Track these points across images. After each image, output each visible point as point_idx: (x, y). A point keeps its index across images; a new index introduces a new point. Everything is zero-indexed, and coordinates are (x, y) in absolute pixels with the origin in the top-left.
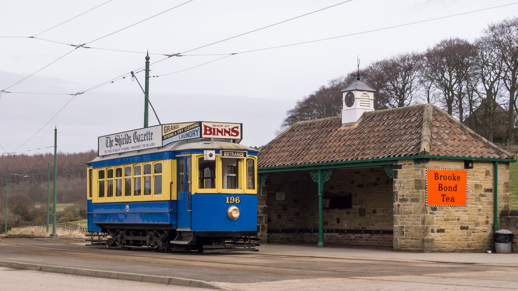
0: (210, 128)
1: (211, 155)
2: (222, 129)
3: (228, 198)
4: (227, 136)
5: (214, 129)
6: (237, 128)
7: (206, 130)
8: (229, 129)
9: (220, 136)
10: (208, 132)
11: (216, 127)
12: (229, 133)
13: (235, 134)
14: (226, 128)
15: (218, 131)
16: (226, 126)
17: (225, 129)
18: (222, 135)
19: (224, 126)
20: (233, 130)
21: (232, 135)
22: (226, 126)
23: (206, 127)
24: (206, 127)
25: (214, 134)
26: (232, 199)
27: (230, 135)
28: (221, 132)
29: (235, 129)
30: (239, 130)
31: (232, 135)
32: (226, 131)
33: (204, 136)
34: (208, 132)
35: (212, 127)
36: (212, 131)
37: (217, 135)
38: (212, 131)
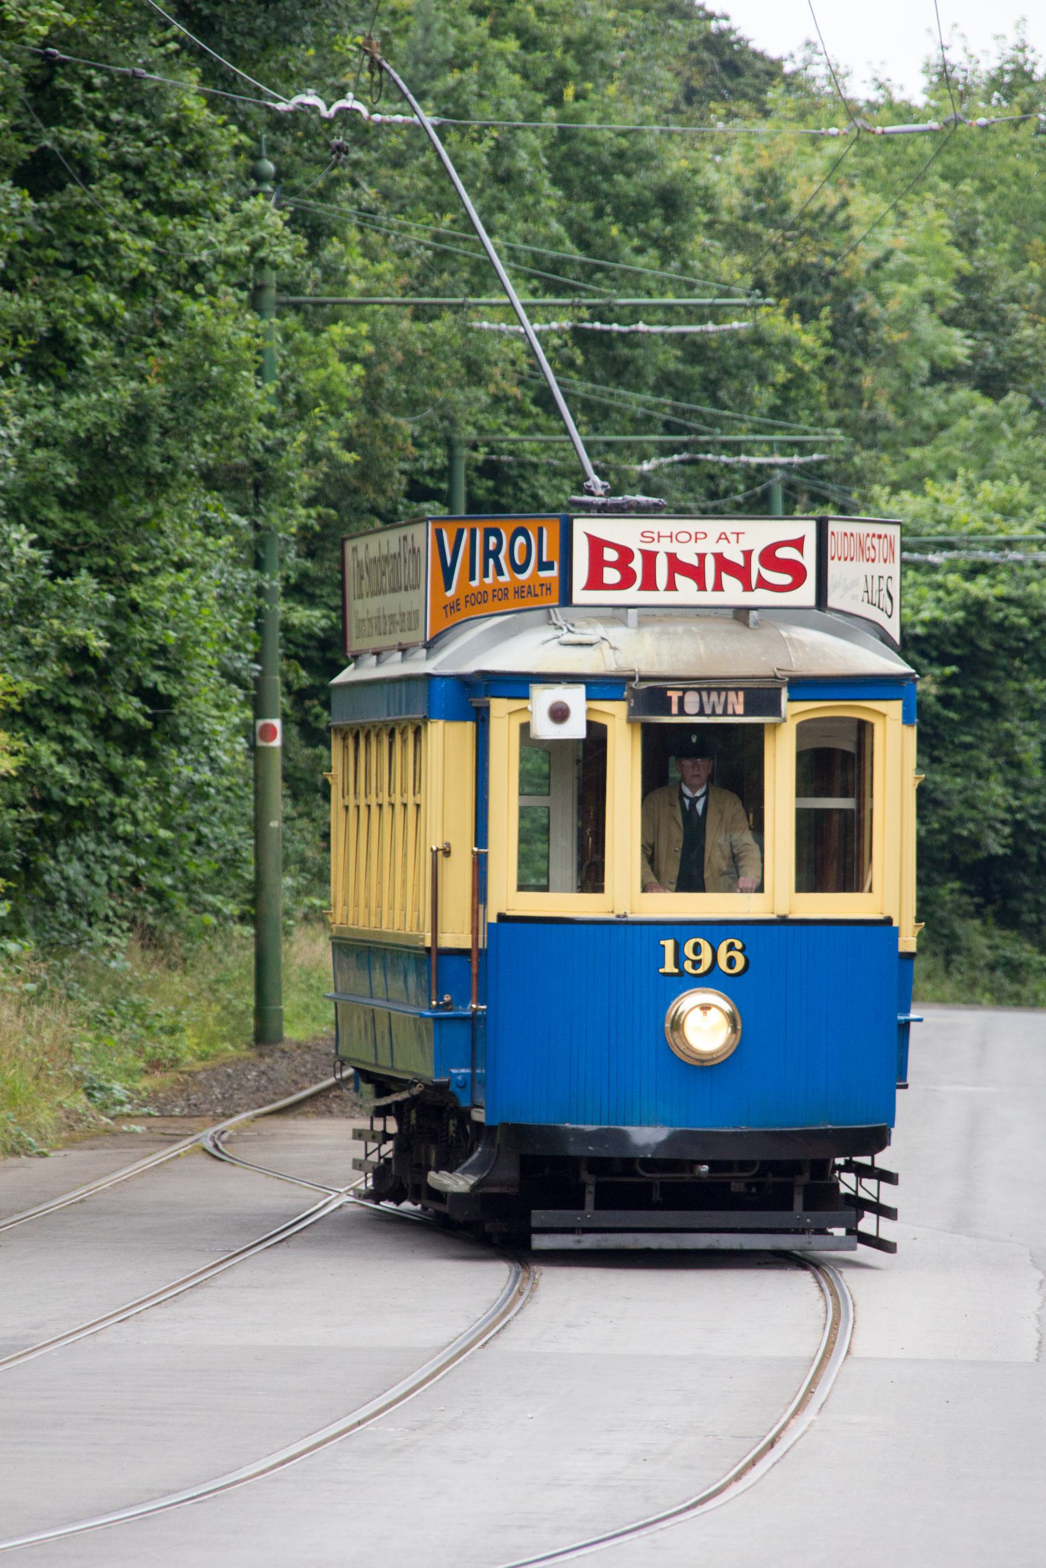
0: (626, 554)
2: (702, 557)
3: (669, 945)
5: (649, 558)
6: (798, 544)
7: (597, 564)
10: (611, 576)
11: (662, 548)
12: (742, 573)
13: (786, 579)
14: (723, 548)
15: (675, 565)
16: (723, 537)
17: (719, 557)
18: (702, 587)
19: (713, 536)
20: (769, 558)
21: (763, 584)
22: (723, 537)
23: (597, 545)
24: (597, 545)
25: (649, 584)
26: (697, 948)
28: (696, 574)
29: (783, 553)
30: (809, 560)
31: (763, 584)
32: (723, 564)
34: (611, 576)
35: (635, 544)
36: (637, 565)
37: (671, 586)
38: (637, 565)
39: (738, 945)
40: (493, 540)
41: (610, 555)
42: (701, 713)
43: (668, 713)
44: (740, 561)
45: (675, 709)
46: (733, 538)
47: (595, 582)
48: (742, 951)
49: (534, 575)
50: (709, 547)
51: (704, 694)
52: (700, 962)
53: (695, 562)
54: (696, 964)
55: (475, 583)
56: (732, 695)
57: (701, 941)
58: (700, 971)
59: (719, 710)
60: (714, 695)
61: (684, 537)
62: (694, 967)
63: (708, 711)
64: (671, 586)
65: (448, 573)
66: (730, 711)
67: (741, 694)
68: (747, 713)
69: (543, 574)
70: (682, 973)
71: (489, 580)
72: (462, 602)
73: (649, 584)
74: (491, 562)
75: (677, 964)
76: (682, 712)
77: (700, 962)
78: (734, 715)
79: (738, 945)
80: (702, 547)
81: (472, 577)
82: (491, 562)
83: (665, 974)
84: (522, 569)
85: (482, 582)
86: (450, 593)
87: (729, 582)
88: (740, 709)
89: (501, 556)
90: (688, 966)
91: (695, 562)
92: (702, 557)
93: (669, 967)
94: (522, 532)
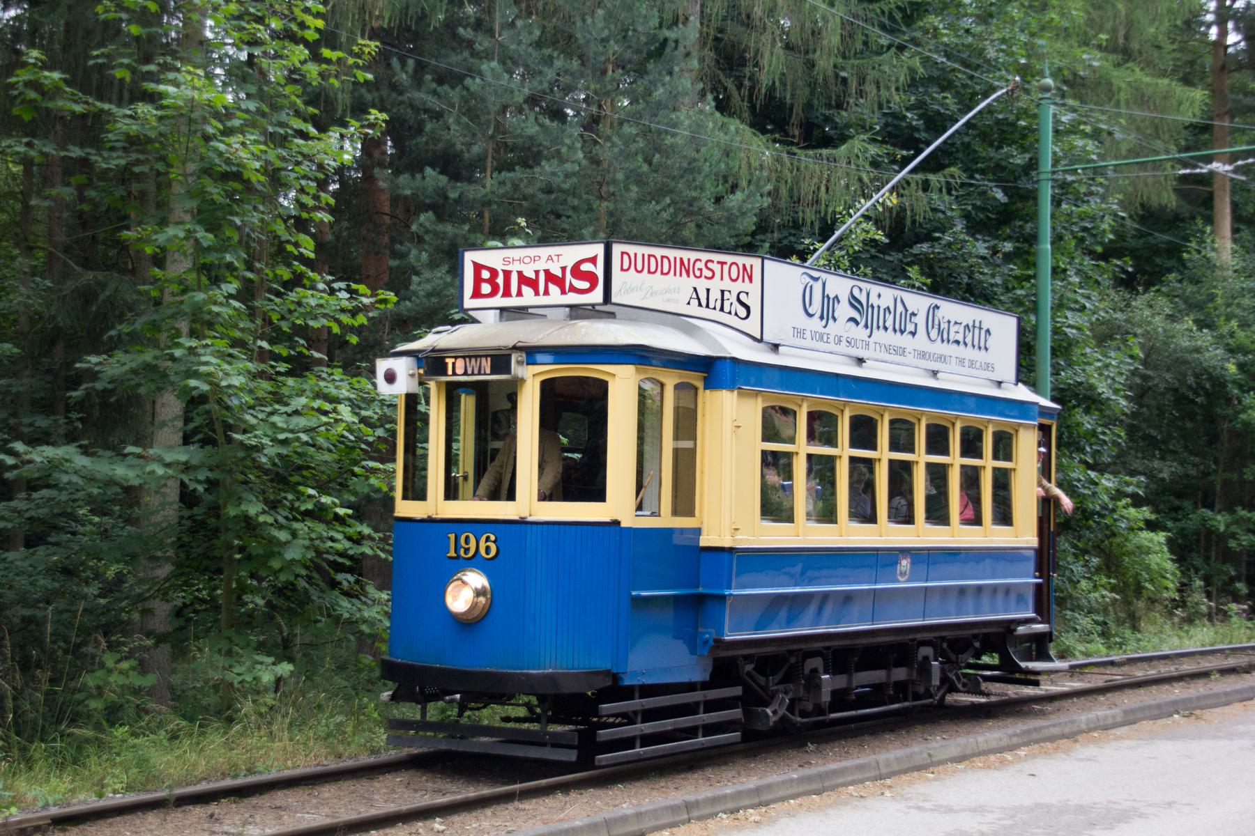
0: (494, 272)
2: (537, 272)
3: (452, 536)
5: (507, 274)
6: (593, 260)
7: (478, 280)
8: (564, 269)
10: (486, 288)
11: (514, 268)
12: (559, 282)
13: (584, 285)
15: (523, 279)
16: (550, 258)
17: (547, 272)
18: (537, 293)
19: (544, 258)
20: (577, 272)
21: (573, 289)
22: (550, 258)
23: (478, 268)
24: (478, 268)
25: (507, 293)
27: (563, 292)
28: (533, 284)
31: (573, 289)
32: (550, 277)
34: (486, 288)
35: (499, 267)
36: (500, 280)
37: (519, 294)
38: (500, 280)
39: (493, 538)
41: (486, 275)
42: (465, 374)
45: (450, 372)
46: (555, 258)
47: (477, 294)
48: (495, 542)
50: (541, 265)
54: (467, 550)
56: (484, 359)
57: (471, 536)
58: (470, 555)
68: (492, 374)
70: (458, 557)
73: (507, 293)
79: (493, 538)
83: (451, 558)
87: (553, 288)
88: (488, 371)
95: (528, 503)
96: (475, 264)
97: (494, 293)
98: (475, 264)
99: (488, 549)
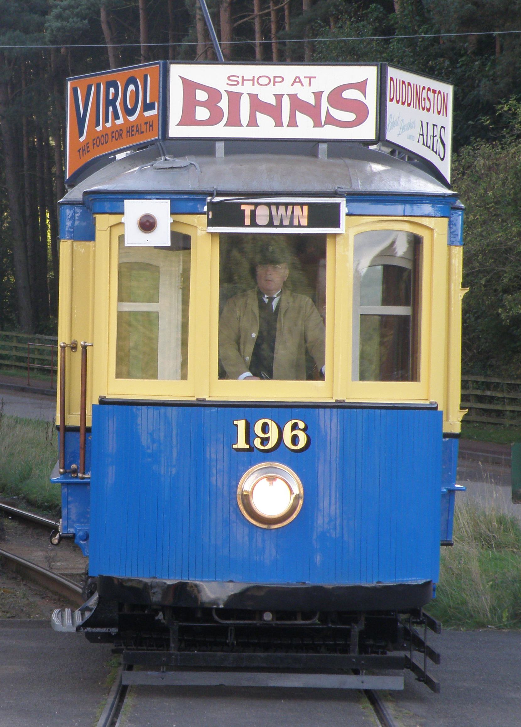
0: (214, 94)
1: (147, 225)
2: (279, 97)
3: (241, 425)
4: (305, 129)
5: (234, 98)
6: (361, 86)
8: (318, 95)
9: (266, 129)
10: (202, 113)
11: (246, 89)
12: (313, 111)
13: (350, 117)
14: (297, 89)
15: (257, 105)
16: (297, 80)
17: (293, 98)
18: (279, 123)
19: (289, 79)
20: (336, 98)
21: (331, 120)
22: (297, 80)
23: (190, 87)
24: (190, 87)
25: (234, 121)
27: (318, 124)
28: (274, 111)
29: (348, 94)
31: (331, 120)
32: (297, 104)
33: (176, 131)
34: (202, 113)
35: (222, 86)
36: (224, 104)
37: (253, 122)
38: (224, 104)
39: (301, 425)
40: (112, 90)
41: (201, 96)
42: (271, 224)
43: (242, 225)
44: (312, 100)
45: (247, 221)
46: (306, 81)
47: (188, 119)
48: (304, 430)
49: (141, 114)
50: (285, 89)
51: (273, 208)
52: (268, 439)
53: (273, 102)
54: (265, 441)
55: (99, 129)
56: (297, 209)
57: (269, 421)
58: (269, 447)
59: (286, 222)
60: (282, 209)
61: (264, 81)
62: (262, 444)
63: (276, 223)
64: (253, 122)
65: (81, 122)
66: (296, 223)
67: (306, 208)
68: (310, 225)
69: (147, 114)
70: (252, 449)
71: (109, 125)
72: (91, 145)
73: (234, 121)
74: (111, 109)
75: (248, 441)
76: (254, 224)
77: (268, 439)
78: (299, 226)
79: (301, 425)
80: (280, 89)
81: (98, 124)
82: (111, 109)
83: (238, 450)
84: (130, 112)
85: (104, 126)
86: (82, 139)
87: (302, 119)
88: (304, 222)
89: (118, 104)
90: (257, 443)
91: (273, 102)
92: (279, 97)
93: (241, 443)
94: (132, 80)
95: (343, 381)
96: (185, 81)
97: (213, 121)
98: (185, 81)
99: (295, 439)
